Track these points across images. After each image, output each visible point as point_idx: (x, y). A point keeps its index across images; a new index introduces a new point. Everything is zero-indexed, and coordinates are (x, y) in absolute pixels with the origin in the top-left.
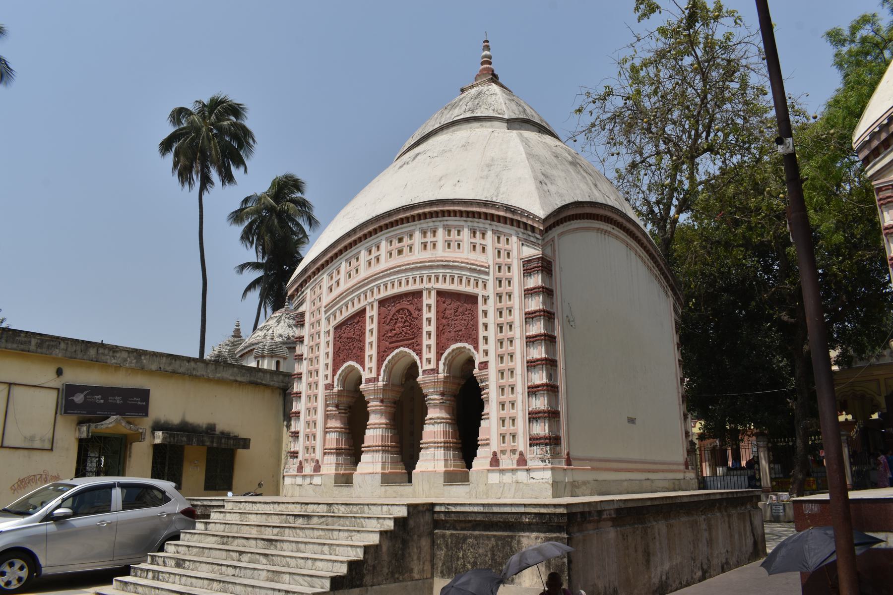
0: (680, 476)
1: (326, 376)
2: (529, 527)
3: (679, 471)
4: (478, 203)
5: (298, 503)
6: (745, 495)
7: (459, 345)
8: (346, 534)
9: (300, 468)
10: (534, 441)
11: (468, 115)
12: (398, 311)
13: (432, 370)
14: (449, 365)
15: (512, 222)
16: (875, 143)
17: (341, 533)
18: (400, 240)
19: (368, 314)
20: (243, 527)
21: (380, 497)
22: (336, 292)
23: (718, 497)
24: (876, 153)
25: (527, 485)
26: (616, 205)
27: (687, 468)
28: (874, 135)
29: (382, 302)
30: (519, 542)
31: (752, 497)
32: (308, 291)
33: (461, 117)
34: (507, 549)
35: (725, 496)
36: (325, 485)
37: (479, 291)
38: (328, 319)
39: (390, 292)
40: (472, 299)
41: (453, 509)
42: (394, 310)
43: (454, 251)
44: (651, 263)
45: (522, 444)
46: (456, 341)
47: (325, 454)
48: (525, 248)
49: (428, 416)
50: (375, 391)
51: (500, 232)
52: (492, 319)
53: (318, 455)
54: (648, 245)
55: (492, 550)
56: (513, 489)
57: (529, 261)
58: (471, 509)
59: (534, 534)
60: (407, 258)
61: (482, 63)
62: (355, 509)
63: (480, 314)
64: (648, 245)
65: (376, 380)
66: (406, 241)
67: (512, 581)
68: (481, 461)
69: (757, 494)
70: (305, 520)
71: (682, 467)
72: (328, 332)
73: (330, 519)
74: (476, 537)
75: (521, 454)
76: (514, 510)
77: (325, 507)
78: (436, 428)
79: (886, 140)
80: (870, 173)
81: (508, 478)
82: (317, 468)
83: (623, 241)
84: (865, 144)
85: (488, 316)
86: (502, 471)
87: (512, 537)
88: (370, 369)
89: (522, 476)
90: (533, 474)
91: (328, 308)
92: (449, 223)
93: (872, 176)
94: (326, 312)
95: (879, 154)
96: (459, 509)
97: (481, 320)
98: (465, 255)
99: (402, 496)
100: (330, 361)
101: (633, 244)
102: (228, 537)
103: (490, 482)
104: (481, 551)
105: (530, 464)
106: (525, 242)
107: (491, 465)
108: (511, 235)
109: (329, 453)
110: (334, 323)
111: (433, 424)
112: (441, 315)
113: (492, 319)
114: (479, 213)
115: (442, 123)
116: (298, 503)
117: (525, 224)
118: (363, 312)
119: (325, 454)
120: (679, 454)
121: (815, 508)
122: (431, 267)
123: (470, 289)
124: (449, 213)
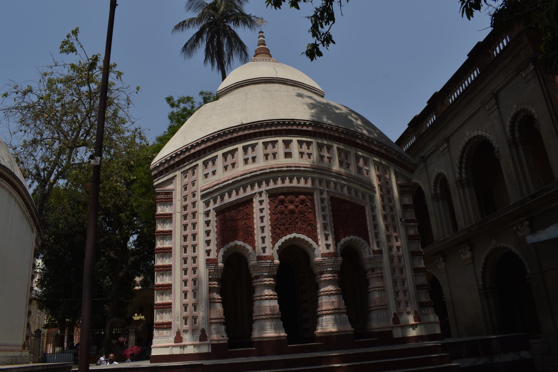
0: (18, 354)
3: (18, 351)
6: (61, 366)
16: (161, 168)
23: (40, 368)
24: (161, 174)
26: (8, 166)
27: (24, 348)
28: (161, 164)
31: (65, 367)
35: (45, 368)
44: (25, 209)
54: (26, 196)
64: (26, 196)
69: (69, 365)
71: (21, 348)
79: (167, 168)
80: (155, 184)
83: (7, 190)
84: (156, 168)
93: (156, 185)
95: (162, 175)
101: (15, 194)
120: (20, 340)
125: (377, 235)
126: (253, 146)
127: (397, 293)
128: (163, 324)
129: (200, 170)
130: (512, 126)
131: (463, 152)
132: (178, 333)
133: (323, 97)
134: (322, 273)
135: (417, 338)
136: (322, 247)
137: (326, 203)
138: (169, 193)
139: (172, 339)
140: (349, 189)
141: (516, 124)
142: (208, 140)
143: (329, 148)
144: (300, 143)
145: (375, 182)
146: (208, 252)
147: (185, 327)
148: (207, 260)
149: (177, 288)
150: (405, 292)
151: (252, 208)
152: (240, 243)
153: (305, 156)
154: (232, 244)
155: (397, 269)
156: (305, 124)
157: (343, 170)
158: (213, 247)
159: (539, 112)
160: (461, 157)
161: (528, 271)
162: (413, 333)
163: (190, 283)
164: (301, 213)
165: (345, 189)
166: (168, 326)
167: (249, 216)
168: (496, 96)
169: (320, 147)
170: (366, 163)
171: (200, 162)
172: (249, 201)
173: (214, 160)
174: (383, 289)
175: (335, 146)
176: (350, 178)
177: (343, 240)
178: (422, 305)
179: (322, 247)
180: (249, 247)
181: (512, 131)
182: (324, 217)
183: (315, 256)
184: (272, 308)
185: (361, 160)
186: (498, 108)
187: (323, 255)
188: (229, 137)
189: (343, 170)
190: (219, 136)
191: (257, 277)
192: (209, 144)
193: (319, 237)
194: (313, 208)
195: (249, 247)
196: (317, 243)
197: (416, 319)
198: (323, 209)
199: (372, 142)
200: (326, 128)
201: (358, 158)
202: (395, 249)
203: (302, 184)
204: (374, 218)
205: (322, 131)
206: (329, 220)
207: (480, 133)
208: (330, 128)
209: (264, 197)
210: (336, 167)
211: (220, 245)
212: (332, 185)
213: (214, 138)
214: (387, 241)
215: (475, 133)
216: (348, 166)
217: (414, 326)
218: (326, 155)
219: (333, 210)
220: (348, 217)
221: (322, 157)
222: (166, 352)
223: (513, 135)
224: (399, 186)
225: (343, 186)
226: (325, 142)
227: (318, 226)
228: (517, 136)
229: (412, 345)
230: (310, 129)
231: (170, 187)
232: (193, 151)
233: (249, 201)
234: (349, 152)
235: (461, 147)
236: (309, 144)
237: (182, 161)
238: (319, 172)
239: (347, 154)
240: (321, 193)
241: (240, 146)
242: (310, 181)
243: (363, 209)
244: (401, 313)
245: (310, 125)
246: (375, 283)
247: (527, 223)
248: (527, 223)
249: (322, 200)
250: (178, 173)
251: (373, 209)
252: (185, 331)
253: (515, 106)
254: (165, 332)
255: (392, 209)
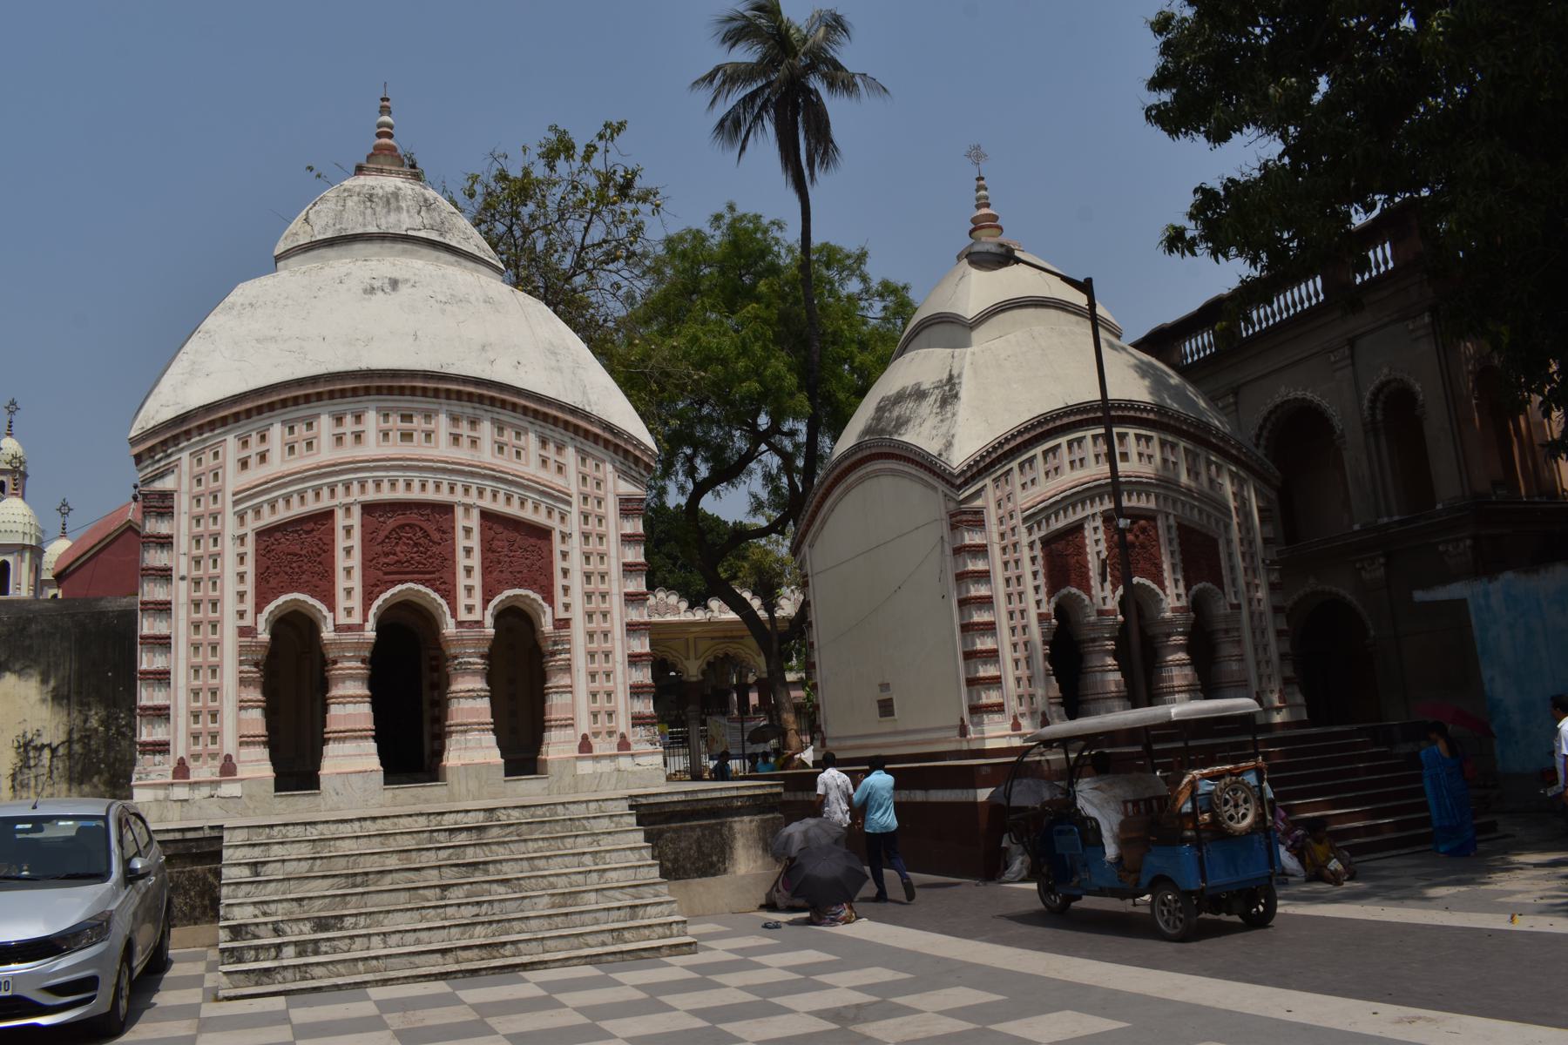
1: (241, 614)
2: (739, 812)
4: (562, 406)
5: (422, 814)
7: (517, 591)
8: (589, 839)
9: (181, 770)
10: (638, 720)
11: (434, 236)
12: (402, 527)
13: (477, 622)
14: (499, 617)
15: (607, 443)
17: (579, 840)
18: (407, 418)
19: (340, 520)
20: (362, 859)
21: (382, 806)
22: (256, 474)
25: (633, 773)
29: (368, 508)
30: (731, 828)
32: (185, 456)
33: (422, 234)
34: (717, 838)
36: (250, 797)
37: (554, 523)
38: (241, 517)
39: (386, 494)
40: (544, 533)
41: (644, 801)
42: (391, 523)
43: (510, 460)
45: (623, 724)
46: (514, 586)
47: (241, 744)
48: (621, 483)
49: (454, 688)
50: (358, 646)
51: (589, 454)
52: (576, 563)
53: (229, 744)
55: (698, 841)
56: (613, 781)
57: (628, 500)
58: (669, 799)
59: (747, 819)
60: (417, 449)
61: (379, 135)
62: (539, 811)
63: (557, 556)
65: (361, 627)
66: (418, 423)
67: (725, 871)
68: (557, 747)
70: (474, 835)
72: (242, 538)
73: (524, 827)
74: (675, 831)
75: (623, 736)
76: (724, 794)
77: (481, 815)
78: (470, 700)
81: (605, 766)
82: (228, 768)
85: (570, 559)
86: (597, 758)
87: (722, 824)
88: (349, 611)
89: (625, 763)
90: (638, 760)
91: (241, 497)
92: (502, 418)
94: (236, 503)
96: (651, 800)
97: (558, 564)
98: (529, 467)
99: (427, 801)
100: (249, 586)
102: (366, 874)
103: (579, 772)
104: (683, 845)
105: (635, 748)
106: (624, 474)
107: (581, 751)
108: (604, 461)
109: (248, 744)
110: (252, 525)
111: (473, 698)
112: (487, 548)
113: (576, 563)
114: (556, 419)
115: (383, 229)
116: (422, 814)
117: (626, 452)
118: (328, 514)
119: (241, 744)
121: (989, 770)
122: (472, 474)
123: (541, 518)
124: (503, 404)
125: (1234, 581)
126: (1080, 440)
127: (1258, 664)
128: (993, 705)
129: (1017, 478)
130: (1373, 401)
131: (1266, 420)
132: (1015, 718)
133: (1119, 337)
134: (1169, 635)
135: (1284, 725)
136: (1172, 598)
137: (1174, 533)
138: (978, 512)
139: (1008, 725)
140: (1200, 511)
141: (1381, 397)
142: (1027, 430)
143: (1173, 446)
144: (1138, 437)
145: (1232, 504)
146: (1038, 603)
147: (1023, 709)
148: (1040, 615)
149: (1007, 655)
150: (1267, 662)
151: (1084, 538)
152: (1074, 590)
153: (1145, 459)
154: (1064, 591)
155: (1258, 631)
156: (1145, 409)
157: (1193, 484)
158: (1043, 595)
159: (1427, 389)
160: (1261, 428)
161: (1372, 633)
162: (1278, 718)
163: (1021, 647)
164: (1143, 546)
165: (1196, 511)
166: (999, 708)
167: (1081, 549)
168: (1351, 343)
169: (1163, 444)
170: (1219, 468)
171: (1015, 464)
172: (1078, 528)
173: (1031, 460)
174: (1241, 659)
175: (1182, 444)
176: (1203, 497)
177: (1195, 588)
178: (1286, 681)
179: (1172, 598)
180: (1085, 597)
181: (1372, 408)
182: (1172, 553)
183: (1161, 610)
184: (1117, 683)
185: (1213, 468)
186: (1353, 364)
187: (1174, 610)
188: (1051, 425)
189: (1193, 484)
190: (1040, 423)
191: (1094, 640)
192: (1027, 436)
193: (1167, 583)
194: (1157, 540)
195: (1085, 597)
196: (1163, 589)
197: (1282, 699)
198: (1170, 541)
199: (1228, 442)
200: (1171, 417)
201: (1209, 463)
202: (1255, 603)
203: (1143, 504)
204: (1230, 555)
205: (1165, 420)
206: (1178, 558)
207: (1309, 395)
208: (1177, 416)
209: (1099, 522)
210: (1184, 479)
211: (1050, 593)
212: (1179, 505)
213: (1033, 427)
214: (1250, 592)
215: (1300, 394)
216: (1197, 475)
217: (1279, 709)
218: (1172, 459)
219: (1180, 544)
220: (1200, 556)
221: (1165, 461)
222: (1003, 744)
223: (1373, 415)
224: (1260, 510)
225: (1192, 507)
226: (1170, 438)
227: (1165, 566)
228: (1379, 417)
229: (1279, 733)
230: (1151, 416)
231: (978, 503)
232: (1007, 447)
233: (1078, 528)
234: (1198, 455)
235: (1264, 411)
236: (1148, 439)
237: (992, 464)
238: (1164, 485)
239: (1196, 456)
240: (1167, 515)
241: (1063, 440)
242: (1153, 498)
243: (1215, 542)
244: (1264, 691)
245: (1152, 410)
246: (1227, 650)
247: (1382, 560)
248: (1382, 560)
249: (1169, 528)
250: (988, 481)
251: (1229, 542)
252: (1022, 715)
253: (1386, 371)
254: (996, 717)
255: (1251, 543)
